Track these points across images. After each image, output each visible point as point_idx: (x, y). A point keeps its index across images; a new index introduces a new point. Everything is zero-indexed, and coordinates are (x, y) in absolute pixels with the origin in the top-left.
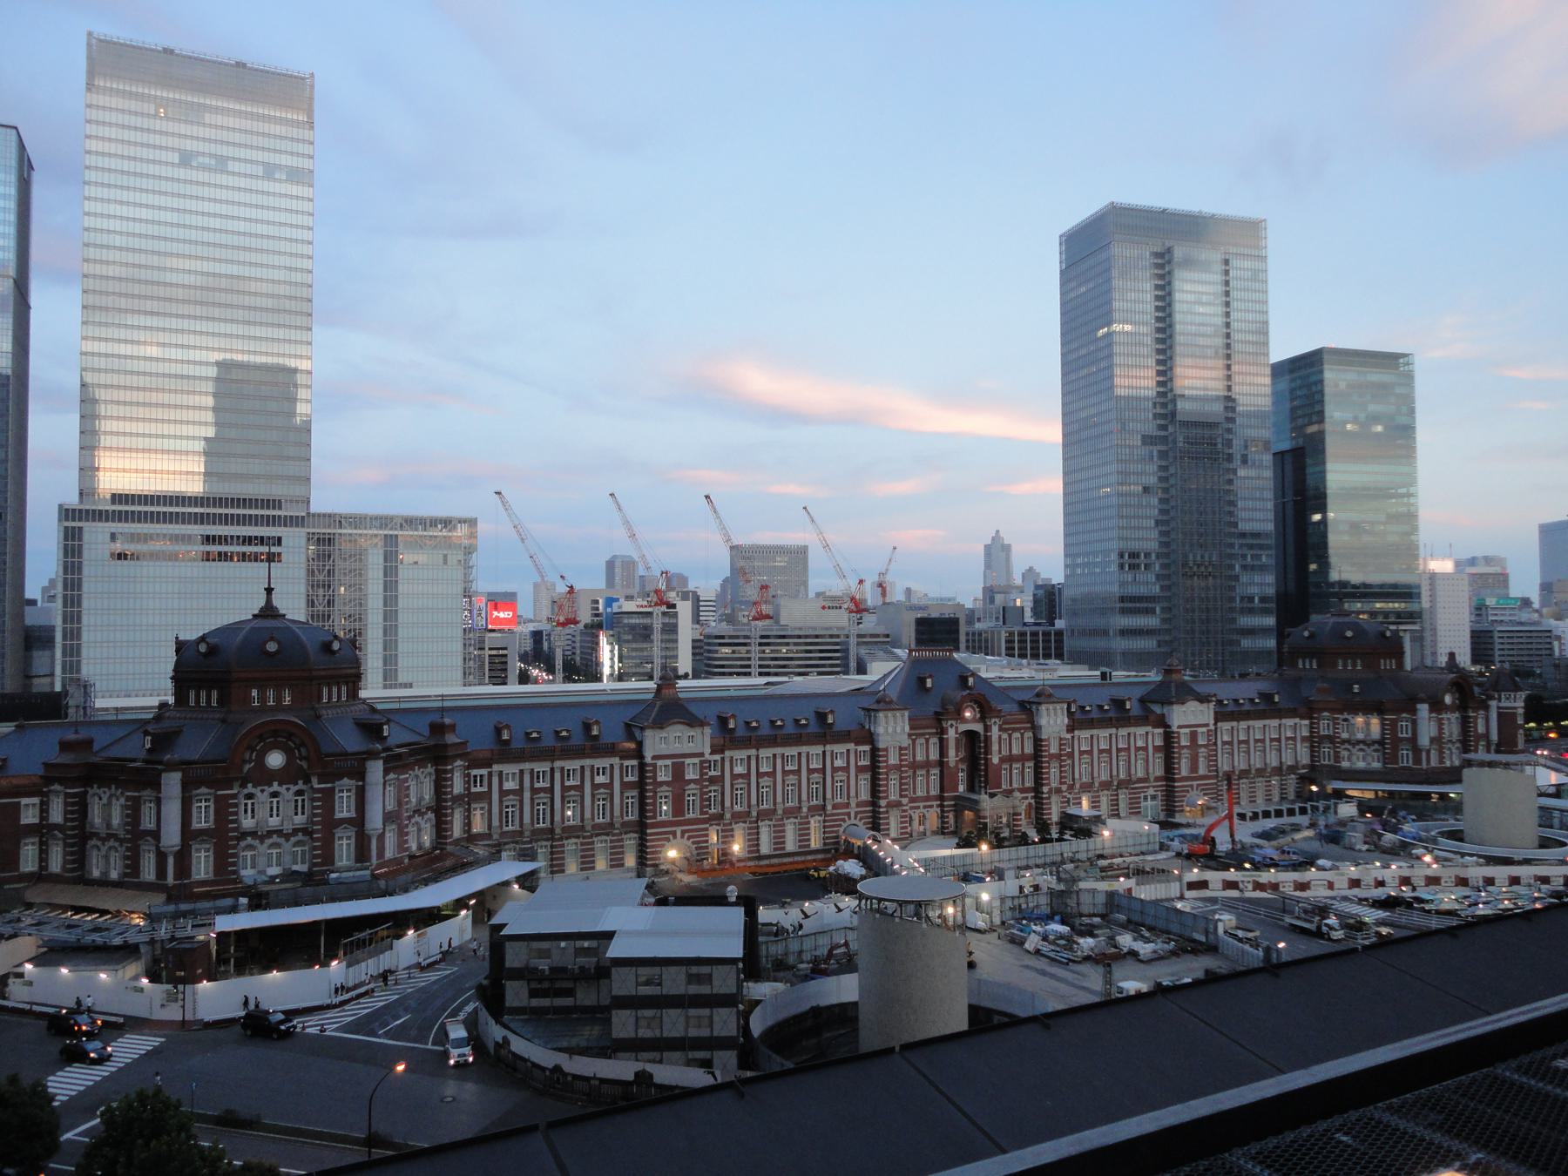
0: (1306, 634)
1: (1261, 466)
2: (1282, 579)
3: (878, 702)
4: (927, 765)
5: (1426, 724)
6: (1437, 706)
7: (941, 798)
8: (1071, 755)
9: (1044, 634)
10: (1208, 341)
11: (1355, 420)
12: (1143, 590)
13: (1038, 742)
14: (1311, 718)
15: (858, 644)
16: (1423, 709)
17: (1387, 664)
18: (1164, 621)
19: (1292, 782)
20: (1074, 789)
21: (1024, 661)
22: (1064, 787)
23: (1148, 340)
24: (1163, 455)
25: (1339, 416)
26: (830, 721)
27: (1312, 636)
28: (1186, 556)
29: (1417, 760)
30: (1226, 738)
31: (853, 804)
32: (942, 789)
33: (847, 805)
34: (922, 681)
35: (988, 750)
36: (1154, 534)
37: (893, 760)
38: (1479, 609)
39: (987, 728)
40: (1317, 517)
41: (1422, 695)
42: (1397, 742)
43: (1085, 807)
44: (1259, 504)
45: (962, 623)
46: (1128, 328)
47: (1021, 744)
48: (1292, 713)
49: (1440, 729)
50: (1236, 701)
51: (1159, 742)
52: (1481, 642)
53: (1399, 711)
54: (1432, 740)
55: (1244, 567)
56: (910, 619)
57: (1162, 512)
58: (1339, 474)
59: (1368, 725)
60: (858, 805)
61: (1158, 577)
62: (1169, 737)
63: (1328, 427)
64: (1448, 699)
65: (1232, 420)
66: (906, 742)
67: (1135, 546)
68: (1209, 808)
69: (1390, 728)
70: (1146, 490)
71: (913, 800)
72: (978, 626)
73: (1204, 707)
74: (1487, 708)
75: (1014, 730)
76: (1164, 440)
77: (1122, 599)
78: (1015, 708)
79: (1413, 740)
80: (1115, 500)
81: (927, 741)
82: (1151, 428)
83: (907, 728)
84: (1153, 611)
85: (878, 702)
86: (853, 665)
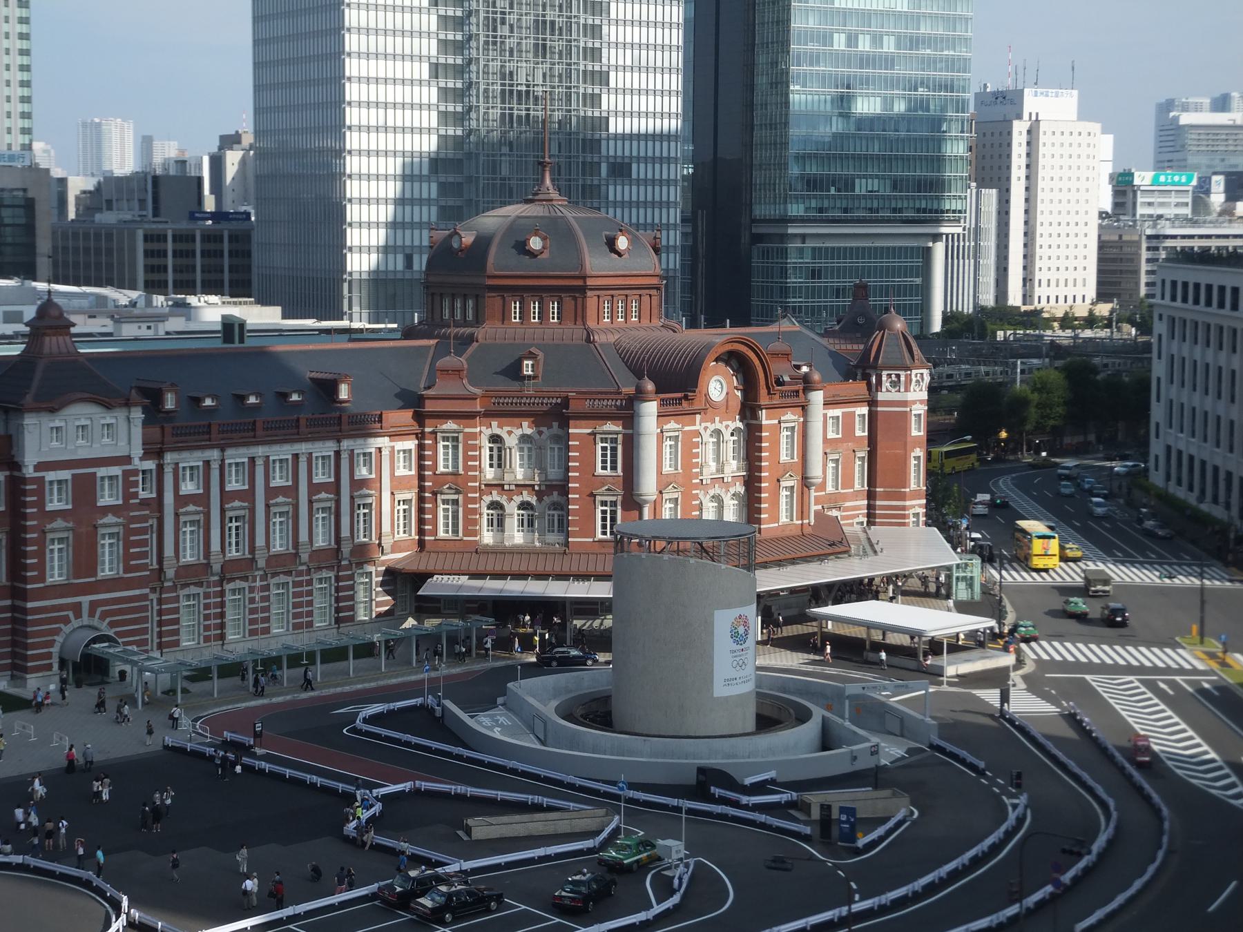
9: (233, 238)
30: (188, 487)
54: (664, 483)
73: (116, 417)
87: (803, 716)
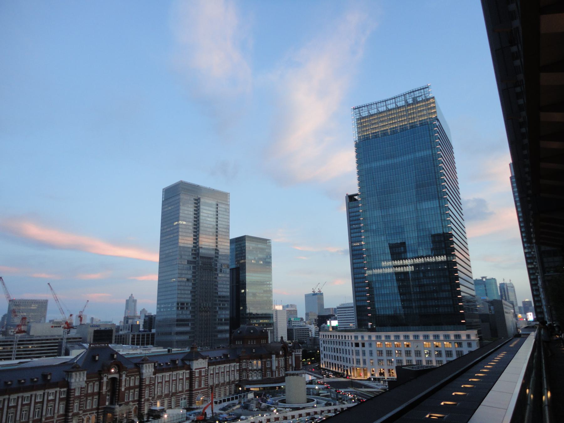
0: (239, 332)
1: (226, 273)
2: (232, 313)
3: (73, 368)
4: (93, 394)
5: (275, 362)
6: (278, 356)
7: (98, 409)
8: (154, 384)
10: (211, 230)
11: (254, 259)
12: (185, 317)
13: (141, 380)
14: (240, 362)
15: (67, 342)
16: (274, 356)
17: (263, 341)
18: (192, 328)
19: (233, 386)
20: (154, 399)
21: (138, 347)
22: (150, 398)
23: (191, 228)
24: (194, 268)
25: (250, 258)
26: (49, 378)
27: (240, 333)
28: (200, 304)
29: (272, 375)
31: (56, 417)
32: (99, 405)
33: (53, 417)
34: (94, 357)
35: (120, 385)
36: (190, 296)
37: (77, 394)
38: (289, 322)
39: (121, 376)
40: (243, 291)
41: (273, 352)
42: (266, 369)
43: (158, 406)
44: (225, 286)
45: (114, 331)
46: (184, 223)
47: (134, 381)
48: (233, 361)
49: (279, 363)
50: (215, 358)
51: (188, 376)
52: (290, 332)
53: (266, 358)
54: (276, 367)
55: (220, 308)
56: (92, 330)
57: (193, 288)
58: (250, 277)
59: (257, 364)
60: (58, 417)
61: (191, 312)
62: (191, 373)
63: (247, 261)
64: (281, 353)
65: (217, 257)
66: (84, 385)
67: (182, 300)
68: (205, 401)
69: (264, 364)
70: (188, 280)
71: (84, 411)
72: (121, 333)
74: (292, 355)
75: (132, 376)
76: (195, 263)
77: (177, 320)
78: (133, 366)
79: (271, 368)
80: (176, 284)
81: (94, 384)
82: (190, 258)
83: (85, 379)
84: (187, 325)
85: (73, 368)
86: (63, 352)
87: (314, 401)
